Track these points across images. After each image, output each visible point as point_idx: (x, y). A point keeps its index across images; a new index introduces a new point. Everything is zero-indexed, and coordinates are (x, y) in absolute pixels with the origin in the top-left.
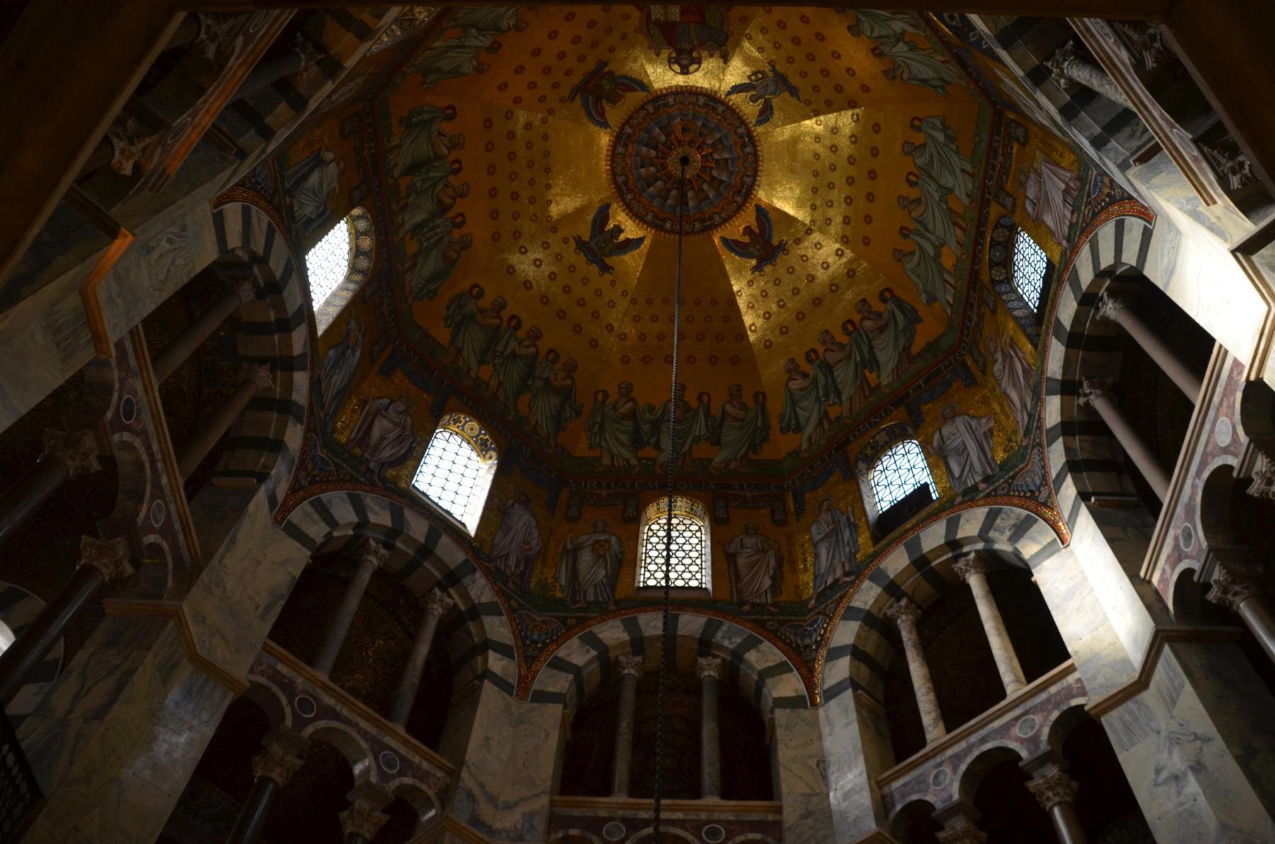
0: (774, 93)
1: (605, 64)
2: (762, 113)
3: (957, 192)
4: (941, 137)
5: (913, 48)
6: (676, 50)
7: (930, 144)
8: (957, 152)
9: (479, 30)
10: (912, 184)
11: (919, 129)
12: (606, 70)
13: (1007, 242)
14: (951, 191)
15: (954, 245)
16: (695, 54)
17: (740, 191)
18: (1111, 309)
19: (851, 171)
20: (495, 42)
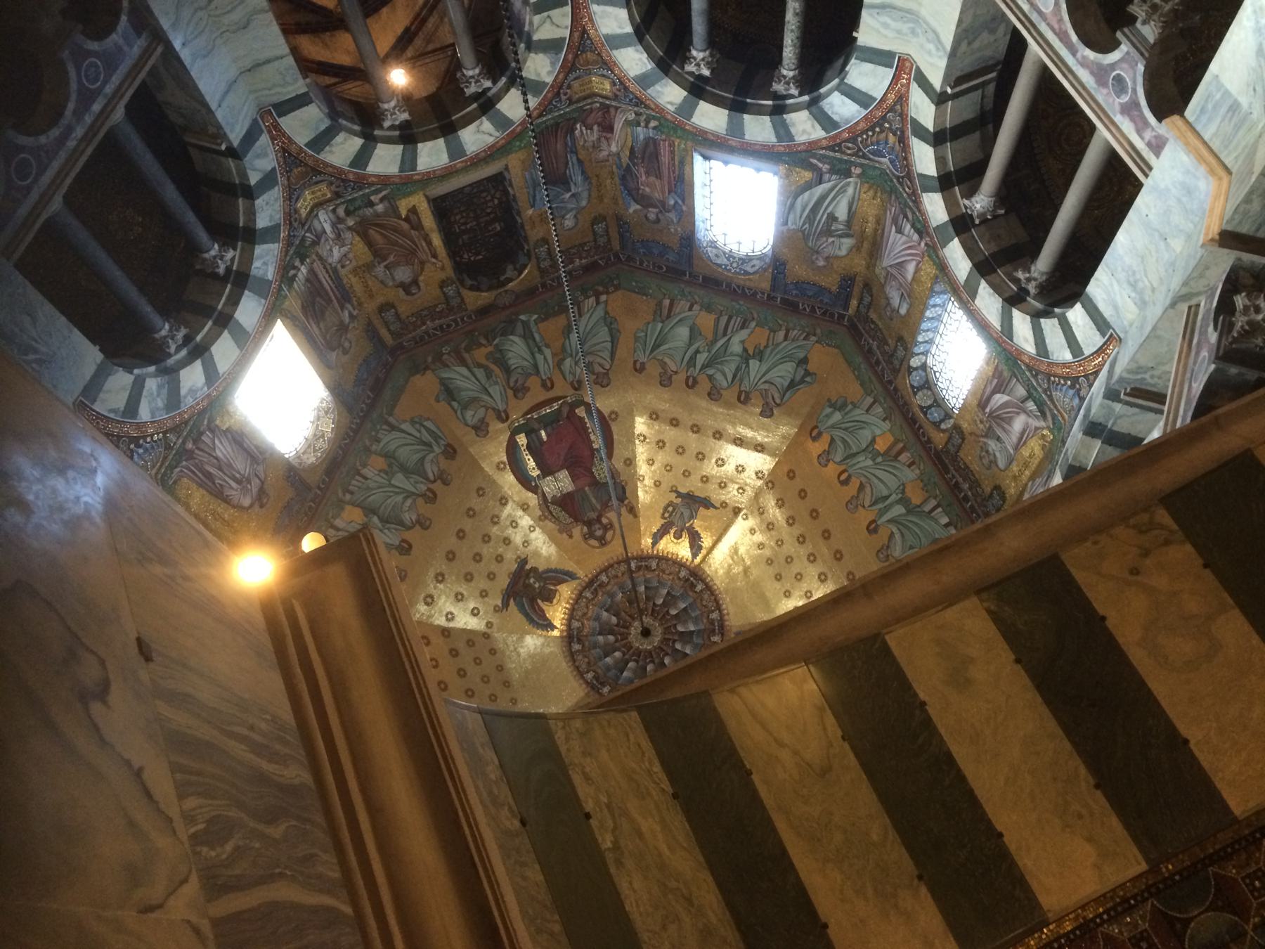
0: (692, 517)
1: (524, 562)
2: (692, 547)
3: (878, 432)
4: (837, 416)
5: (760, 355)
6: (585, 523)
7: (838, 433)
8: (855, 406)
9: (385, 521)
10: (845, 483)
11: (820, 434)
12: (528, 567)
13: (935, 401)
14: (873, 441)
15: (910, 475)
16: (604, 521)
17: (714, 631)
18: (980, 203)
19: (797, 530)
20: (404, 541)
